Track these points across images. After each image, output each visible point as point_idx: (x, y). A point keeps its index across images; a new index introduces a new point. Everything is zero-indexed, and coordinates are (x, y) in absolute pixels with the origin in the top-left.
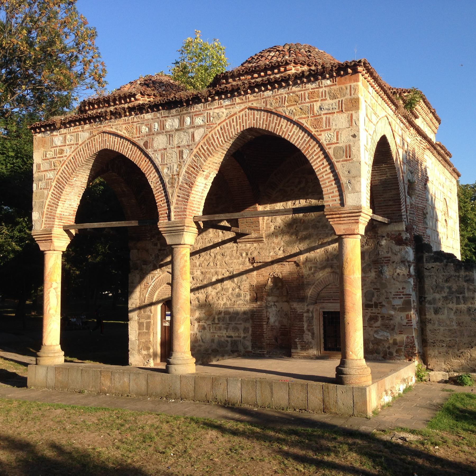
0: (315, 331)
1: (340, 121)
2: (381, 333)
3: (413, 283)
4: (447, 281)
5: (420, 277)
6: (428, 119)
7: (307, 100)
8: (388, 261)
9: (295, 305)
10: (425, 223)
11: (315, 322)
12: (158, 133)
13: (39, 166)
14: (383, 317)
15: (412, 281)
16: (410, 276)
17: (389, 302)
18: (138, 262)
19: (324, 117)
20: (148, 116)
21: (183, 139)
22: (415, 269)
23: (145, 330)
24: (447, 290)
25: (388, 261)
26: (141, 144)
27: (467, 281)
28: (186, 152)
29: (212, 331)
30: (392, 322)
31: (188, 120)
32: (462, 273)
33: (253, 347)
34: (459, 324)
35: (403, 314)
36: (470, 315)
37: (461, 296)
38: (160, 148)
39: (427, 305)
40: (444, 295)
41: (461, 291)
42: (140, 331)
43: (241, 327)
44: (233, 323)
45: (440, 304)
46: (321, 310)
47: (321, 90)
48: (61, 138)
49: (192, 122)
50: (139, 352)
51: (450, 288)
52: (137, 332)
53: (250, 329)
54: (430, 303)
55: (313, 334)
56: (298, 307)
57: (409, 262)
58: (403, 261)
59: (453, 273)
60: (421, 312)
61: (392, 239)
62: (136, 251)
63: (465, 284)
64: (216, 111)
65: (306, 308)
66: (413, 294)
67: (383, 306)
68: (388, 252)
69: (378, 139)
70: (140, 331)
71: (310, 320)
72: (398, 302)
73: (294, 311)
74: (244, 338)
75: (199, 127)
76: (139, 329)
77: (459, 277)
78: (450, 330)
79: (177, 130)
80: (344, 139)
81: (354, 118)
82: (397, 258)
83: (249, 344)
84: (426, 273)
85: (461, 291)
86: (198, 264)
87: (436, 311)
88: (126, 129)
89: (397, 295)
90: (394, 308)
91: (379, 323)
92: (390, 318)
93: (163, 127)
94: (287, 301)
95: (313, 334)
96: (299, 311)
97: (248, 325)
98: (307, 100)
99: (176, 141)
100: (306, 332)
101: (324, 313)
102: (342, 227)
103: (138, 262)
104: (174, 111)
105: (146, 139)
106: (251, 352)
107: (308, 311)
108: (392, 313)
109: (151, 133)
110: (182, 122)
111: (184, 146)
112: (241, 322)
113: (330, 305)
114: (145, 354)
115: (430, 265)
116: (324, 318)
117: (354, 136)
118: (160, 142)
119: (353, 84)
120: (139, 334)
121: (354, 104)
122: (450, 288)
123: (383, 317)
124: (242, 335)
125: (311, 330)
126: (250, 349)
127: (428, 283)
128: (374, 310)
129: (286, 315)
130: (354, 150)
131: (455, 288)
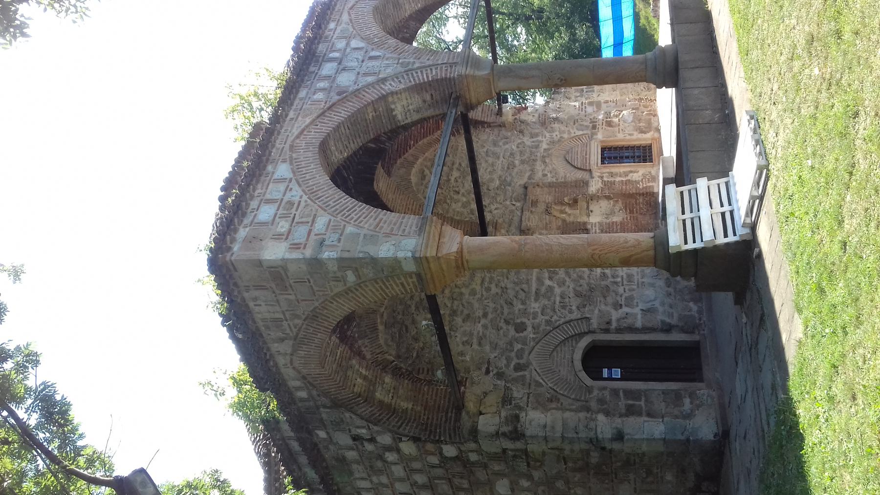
18: (503, 414)
23: (642, 403)
29: (635, 287)
42: (644, 413)
50: (688, 416)
52: (646, 419)
55: (631, 172)
62: (481, 417)
70: (644, 413)
71: (612, 175)
76: (640, 414)
86: (521, 307)
95: (631, 172)
100: (629, 178)
103: (503, 414)
114: (691, 403)
120: (649, 415)
125: (626, 174)
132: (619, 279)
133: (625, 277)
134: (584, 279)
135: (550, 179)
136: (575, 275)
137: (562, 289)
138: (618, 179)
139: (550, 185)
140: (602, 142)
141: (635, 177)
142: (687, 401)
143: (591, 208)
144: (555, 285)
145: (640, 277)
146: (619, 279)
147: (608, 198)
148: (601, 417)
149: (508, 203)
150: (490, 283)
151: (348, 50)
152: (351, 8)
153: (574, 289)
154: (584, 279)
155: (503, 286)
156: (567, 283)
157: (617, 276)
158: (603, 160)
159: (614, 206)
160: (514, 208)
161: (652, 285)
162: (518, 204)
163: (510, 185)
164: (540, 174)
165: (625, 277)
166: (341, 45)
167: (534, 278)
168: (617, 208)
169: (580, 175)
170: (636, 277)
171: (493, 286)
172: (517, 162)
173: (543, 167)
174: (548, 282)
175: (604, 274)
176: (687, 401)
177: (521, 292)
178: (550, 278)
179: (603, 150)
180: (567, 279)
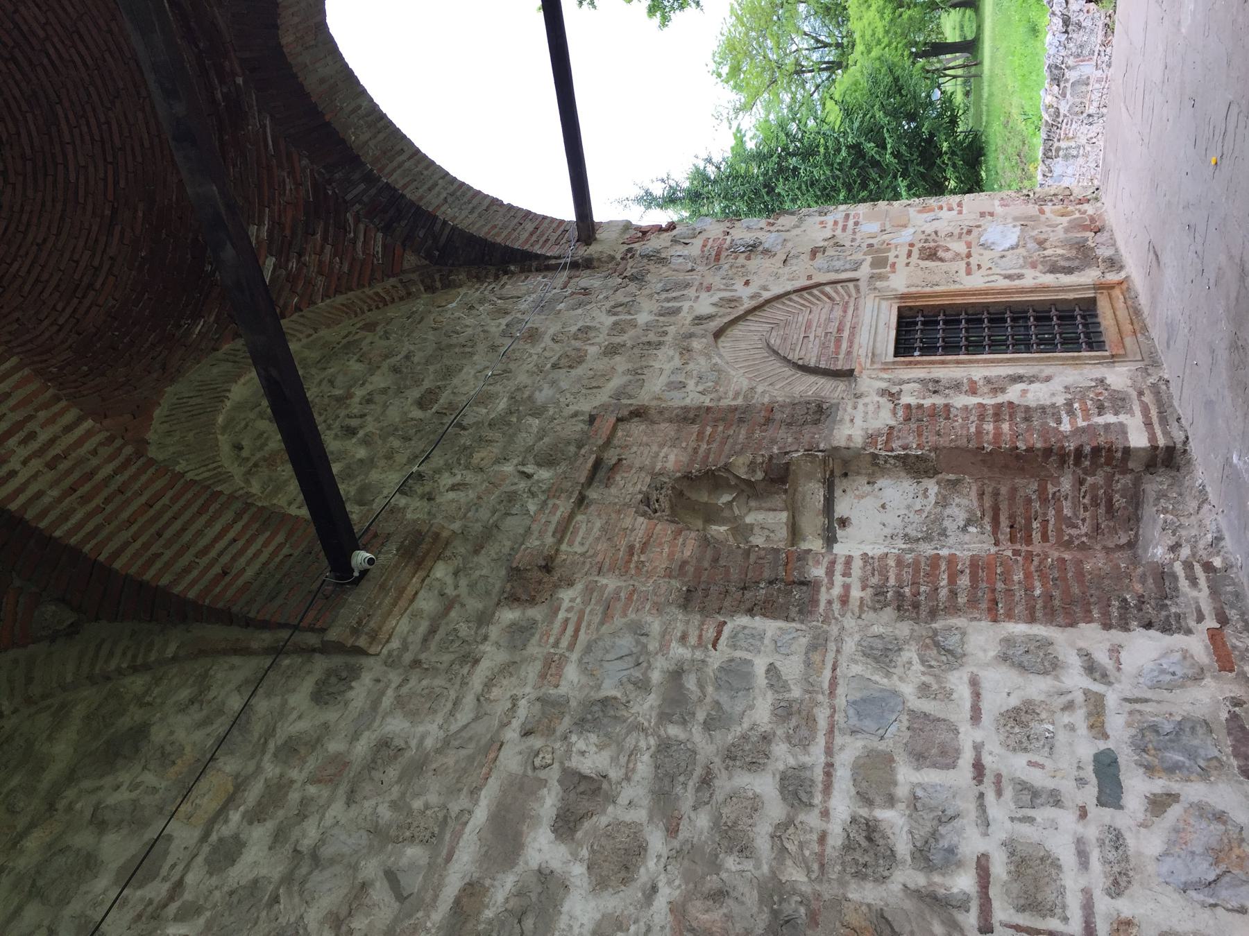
43: (1004, 688)
44: (968, 736)
53: (1019, 629)
71: (935, 387)
83: (1143, 649)
97: (982, 638)
106: (1214, 635)
107: (893, 396)
112: (958, 682)
113: (863, 338)
124: (1075, 680)
125: (996, 387)
132: (964, 882)
133: (999, 868)
134: (746, 851)
135: (692, 396)
136: (703, 821)
137: (611, 902)
138: (961, 401)
139: (689, 417)
140: (903, 297)
141: (1037, 394)
143: (842, 508)
144: (578, 870)
145: (1097, 876)
146: (964, 882)
147: (916, 467)
149: (508, 468)
150: (256, 816)
153: (678, 910)
154: (746, 851)
155: (306, 844)
156: (650, 867)
157: (951, 859)
158: (903, 347)
159: (943, 502)
160: (523, 485)
163: (538, 412)
165: (999, 868)
167: (480, 815)
168: (957, 511)
169: (809, 387)
170: (1072, 881)
171: (259, 834)
173: (677, 362)
174: (542, 848)
175: (871, 830)
177: (380, 893)
178: (566, 825)
179: (906, 321)
180: (656, 841)
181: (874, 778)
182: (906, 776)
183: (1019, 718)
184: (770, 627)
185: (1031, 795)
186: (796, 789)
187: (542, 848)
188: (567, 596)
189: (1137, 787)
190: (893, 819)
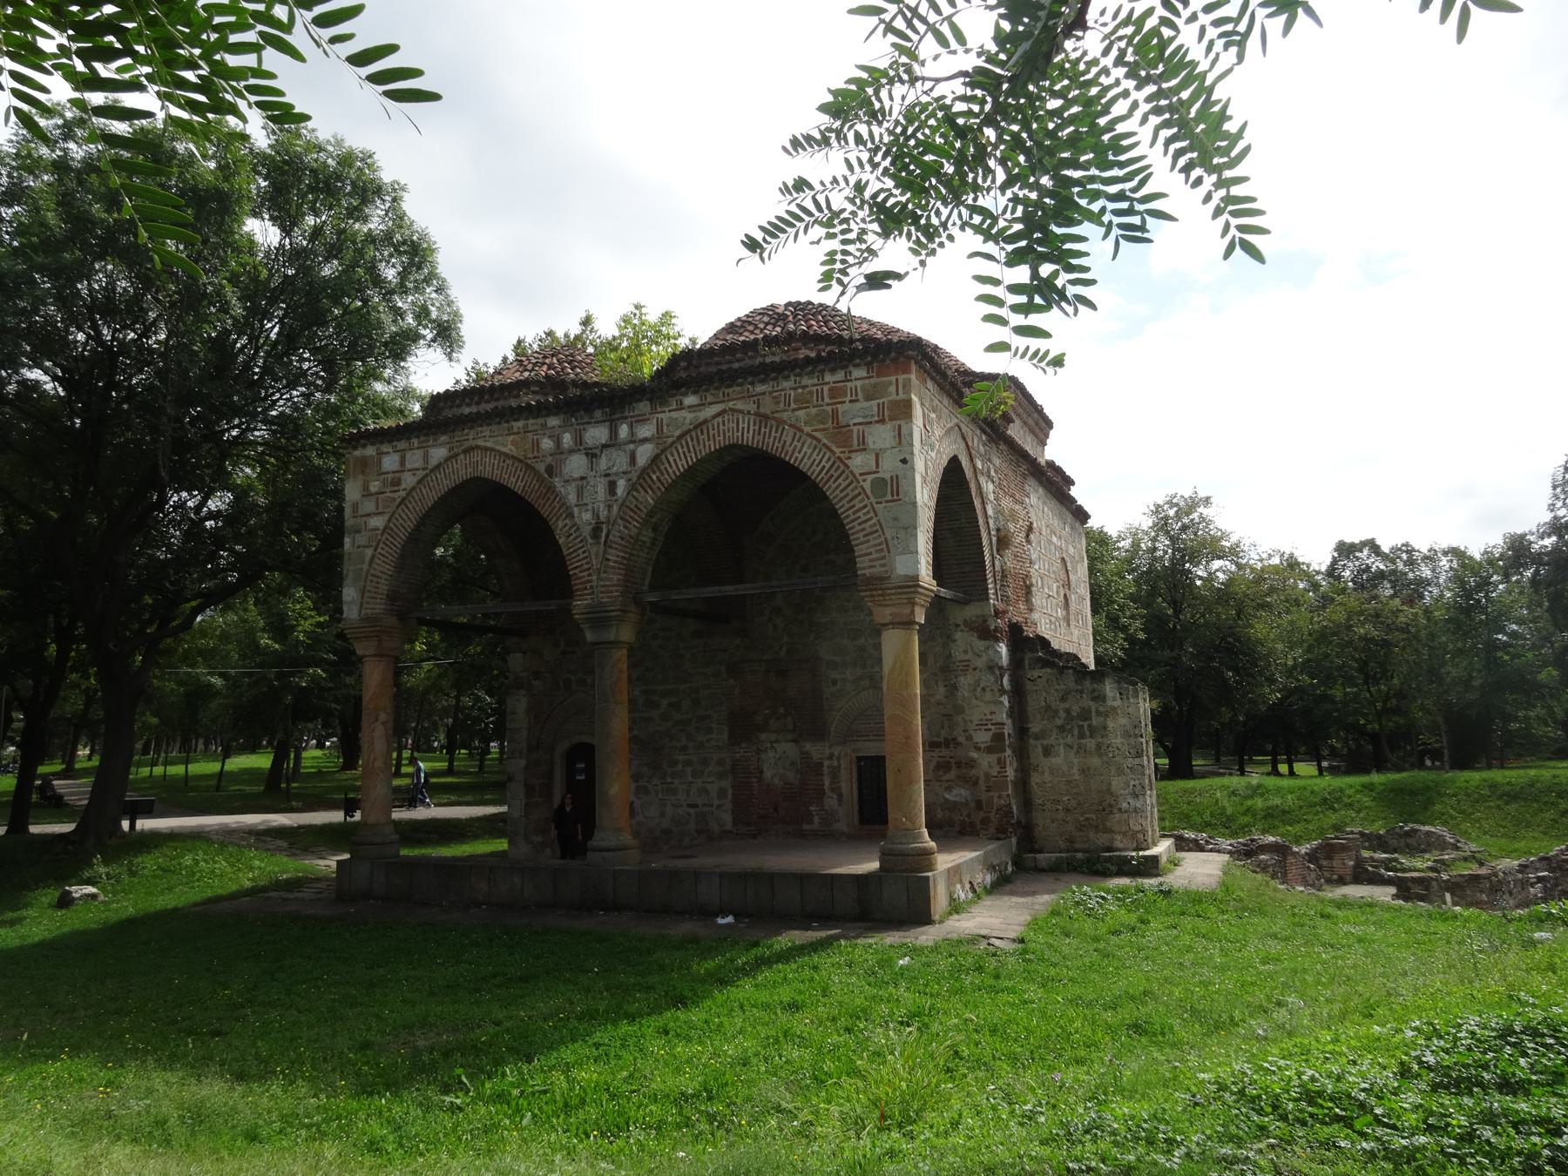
0: (844, 790)
1: (880, 436)
2: (955, 792)
3: (1007, 704)
4: (1063, 699)
5: (1018, 693)
6: (1030, 421)
7: (827, 400)
8: (967, 667)
9: (808, 746)
10: (1028, 601)
11: (844, 774)
12: (571, 451)
13: (355, 506)
14: (959, 764)
15: (1005, 700)
16: (1002, 691)
17: (969, 738)
19: (855, 429)
20: (553, 422)
21: (619, 461)
22: (1011, 681)
24: (1062, 714)
25: (967, 667)
26: (541, 467)
27: (1095, 699)
28: (621, 485)
30: (974, 772)
31: (624, 431)
32: (1088, 683)
33: (735, 823)
34: (1083, 771)
35: (993, 758)
36: (1100, 756)
37: (1086, 724)
38: (576, 475)
39: (1032, 741)
40: (1059, 722)
41: (1085, 715)
45: (1052, 741)
46: (854, 755)
47: (849, 384)
48: (396, 457)
49: (632, 433)
51: (1068, 711)
54: (1037, 737)
55: (840, 796)
56: (815, 750)
57: (1001, 668)
58: (993, 667)
59: (1072, 685)
60: (1022, 754)
61: (971, 629)
63: (1092, 703)
64: (674, 415)
65: (828, 752)
66: (1009, 722)
67: (960, 744)
68: (966, 652)
69: (944, 462)
71: (835, 773)
72: (983, 737)
73: (806, 756)
74: (719, 806)
75: (645, 440)
77: (1081, 692)
78: (1069, 782)
79: (605, 446)
80: (889, 466)
81: (904, 431)
82: (981, 663)
83: (727, 818)
84: (1029, 686)
85: (1085, 715)
87: (1047, 752)
88: (513, 443)
89: (982, 725)
90: (978, 749)
91: (952, 775)
92: (971, 764)
93: (579, 439)
94: (795, 741)
95: (840, 796)
96: (816, 757)
97: (726, 783)
98: (827, 400)
99: (603, 463)
100: (829, 793)
101: (859, 759)
102: (888, 611)
104: (598, 414)
105: (549, 459)
107: (831, 757)
108: (975, 755)
109: (559, 449)
110: (614, 433)
111: (616, 474)
115: (1036, 674)
116: (859, 768)
117: (904, 461)
118: (576, 465)
119: (901, 378)
121: (903, 410)
122: (1068, 711)
123: (959, 764)
124: (716, 802)
125: (836, 789)
126: (729, 827)
127: (1034, 703)
128: (945, 752)
129: (793, 763)
130: (903, 482)
131: (1075, 710)
142: (539, 839)
148: (523, 762)
149: (785, 639)
151: (632, 446)
152: (732, 410)
161: (662, 814)
162: (783, 653)
164: (835, 675)
166: (646, 431)
172: (862, 641)
174: (664, 702)
176: (539, 839)
178: (670, 705)
181: (688, 763)
182: (689, 770)
183: (706, 790)
184: (725, 736)
185: (688, 792)
186: (684, 749)
187: (664, 702)
188: (732, 682)
189: (692, 811)
190: (680, 767)
